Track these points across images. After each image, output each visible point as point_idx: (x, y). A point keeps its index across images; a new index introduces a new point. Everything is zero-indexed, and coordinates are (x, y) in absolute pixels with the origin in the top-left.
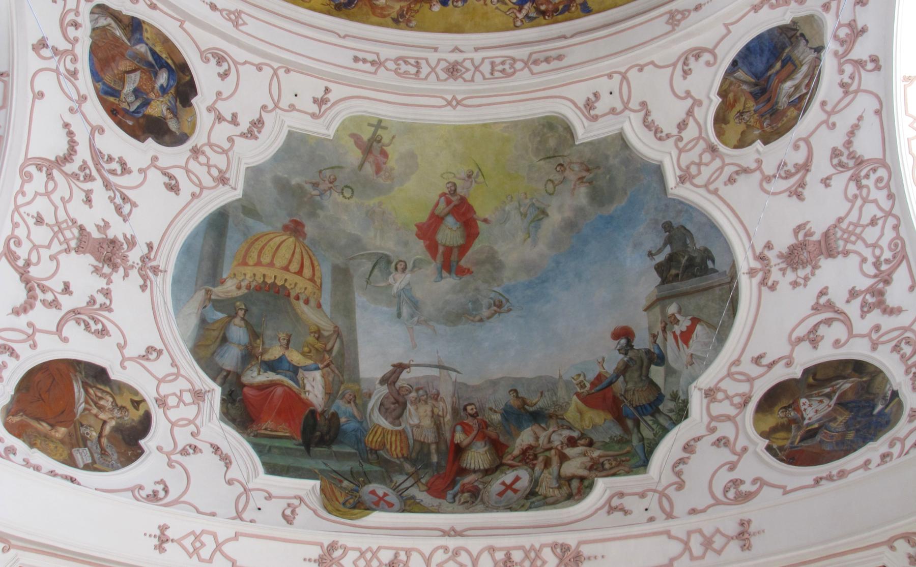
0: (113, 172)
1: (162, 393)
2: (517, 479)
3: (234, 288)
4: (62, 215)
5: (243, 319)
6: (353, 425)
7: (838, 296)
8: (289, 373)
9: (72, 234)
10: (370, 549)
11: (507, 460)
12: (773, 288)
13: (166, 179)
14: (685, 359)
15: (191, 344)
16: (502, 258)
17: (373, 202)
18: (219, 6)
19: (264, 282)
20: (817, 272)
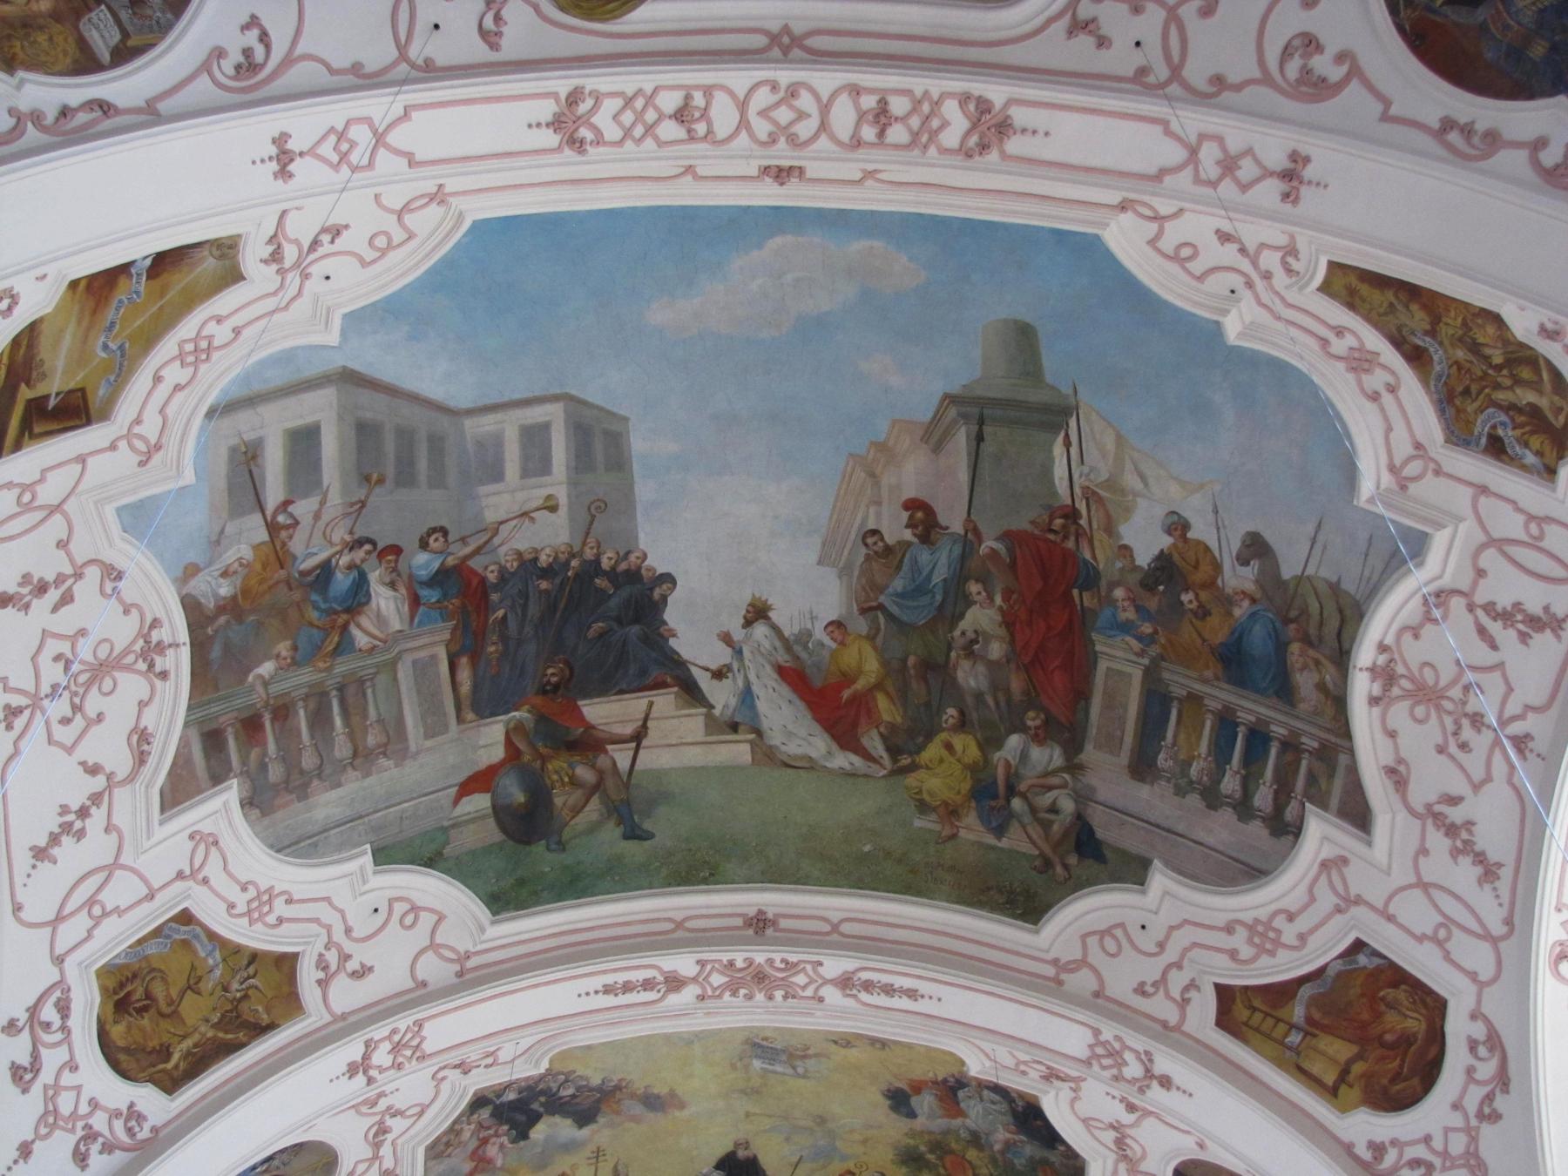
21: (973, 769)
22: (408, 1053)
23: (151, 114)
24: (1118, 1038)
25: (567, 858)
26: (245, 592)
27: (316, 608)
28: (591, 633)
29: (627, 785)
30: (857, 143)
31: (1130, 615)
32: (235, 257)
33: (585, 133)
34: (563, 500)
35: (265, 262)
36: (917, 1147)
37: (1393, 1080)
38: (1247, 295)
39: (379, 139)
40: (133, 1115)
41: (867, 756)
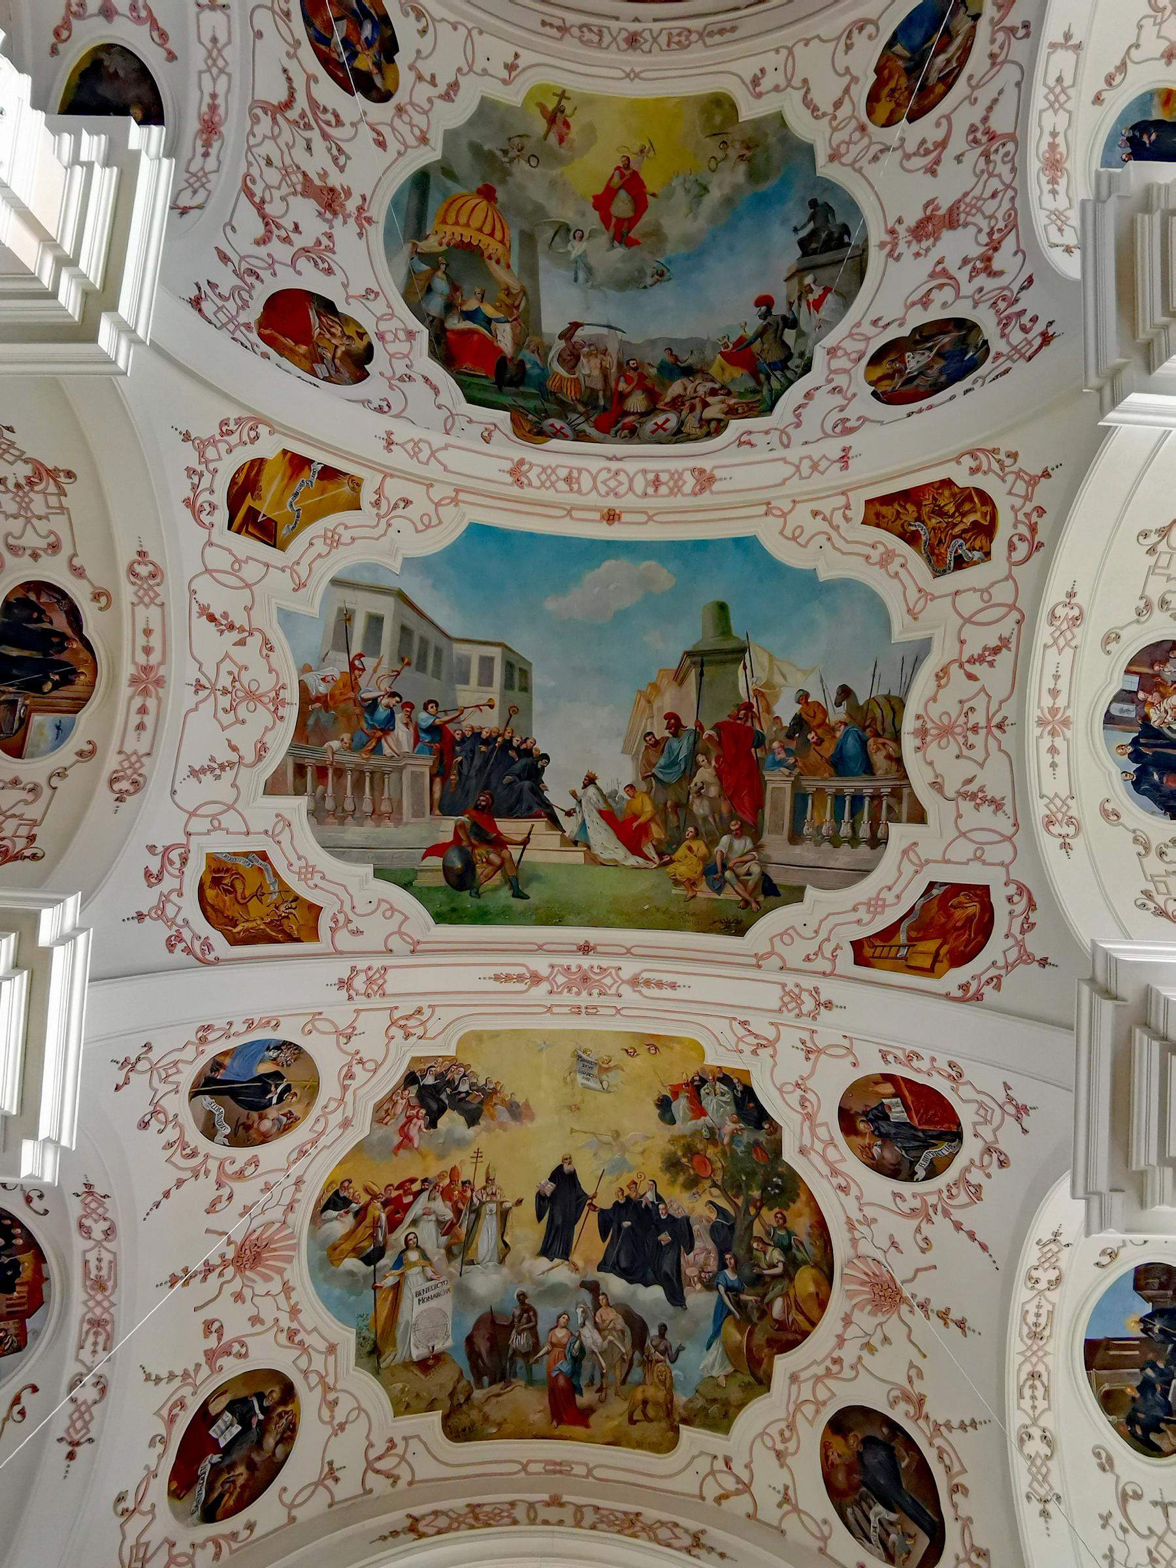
0: (328, 123)
1: (381, 329)
2: (667, 420)
3: (436, 244)
4: (288, 161)
7: (952, 265)
9: (297, 178)
10: (547, 489)
11: (660, 406)
12: (898, 259)
13: (375, 136)
17: (555, 173)
20: (938, 243)
21: (703, 859)
22: (376, 988)
24: (797, 986)
25: (480, 902)
26: (332, 696)
27: (367, 722)
28: (505, 782)
29: (517, 868)
31: (783, 755)
32: (358, 493)
33: (523, 479)
36: (675, 1153)
37: (965, 947)
38: (827, 546)
40: (207, 946)
41: (646, 858)
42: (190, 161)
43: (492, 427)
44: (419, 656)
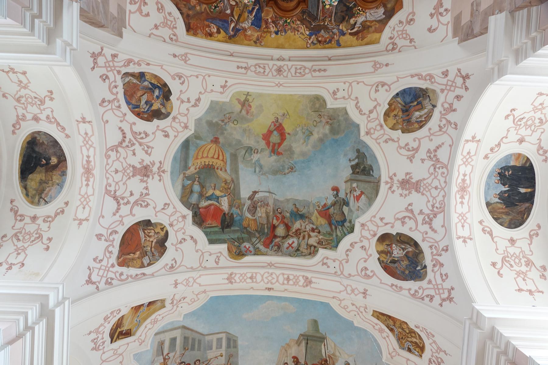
2: (293, 242)
3: (194, 169)
5: (198, 181)
6: (238, 218)
8: (215, 200)
9: (130, 171)
11: (290, 233)
12: (393, 192)
13: (164, 133)
14: (356, 207)
15: (179, 197)
16: (294, 149)
17: (245, 126)
18: (177, 55)
19: (205, 164)
23: (153, 275)
30: (283, 284)
33: (233, 281)
34: (224, 354)
35: (170, 304)
38: (357, 316)
39: (195, 281)
42: (80, 188)
43: (219, 255)
44: (192, 345)
